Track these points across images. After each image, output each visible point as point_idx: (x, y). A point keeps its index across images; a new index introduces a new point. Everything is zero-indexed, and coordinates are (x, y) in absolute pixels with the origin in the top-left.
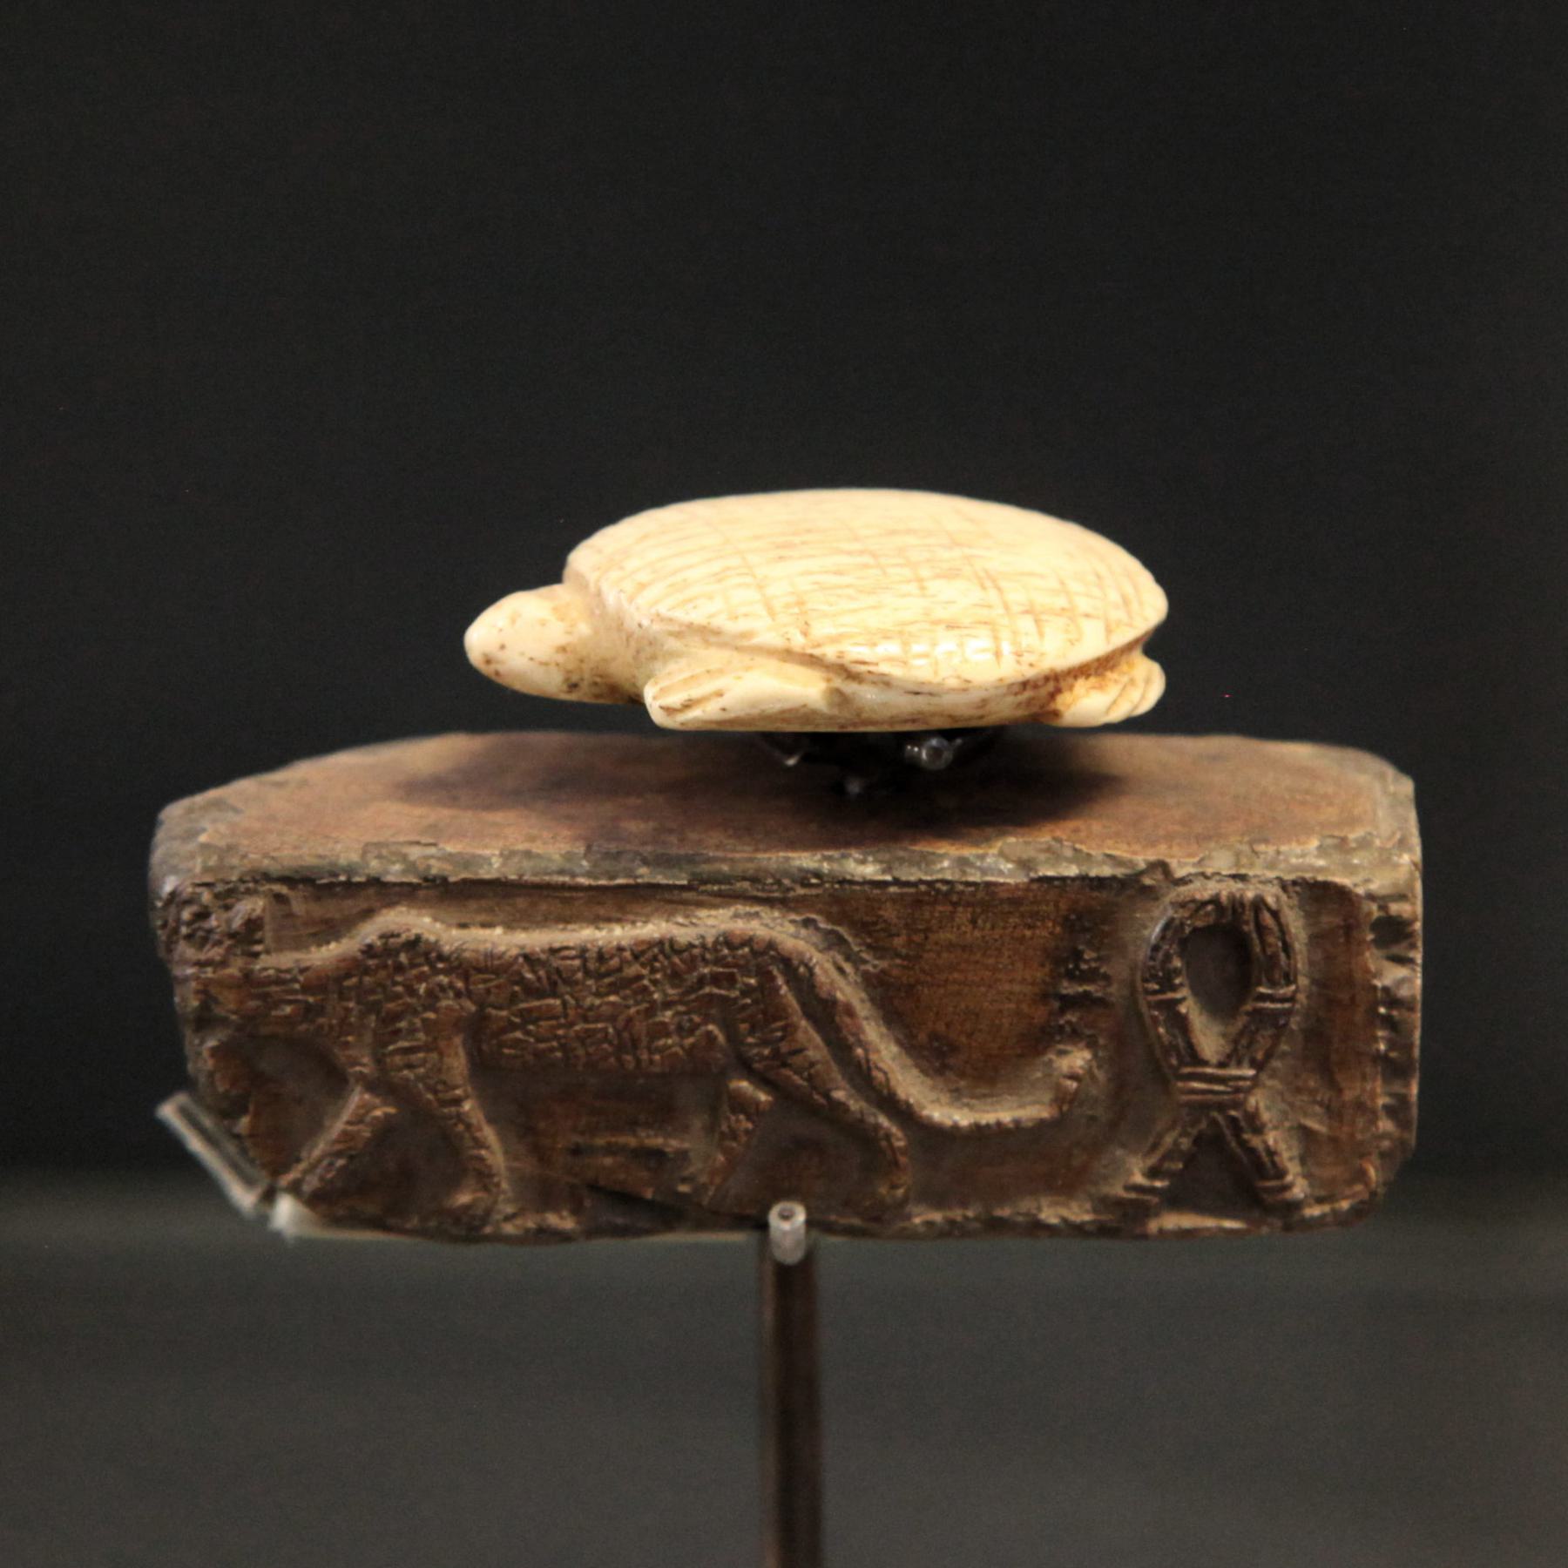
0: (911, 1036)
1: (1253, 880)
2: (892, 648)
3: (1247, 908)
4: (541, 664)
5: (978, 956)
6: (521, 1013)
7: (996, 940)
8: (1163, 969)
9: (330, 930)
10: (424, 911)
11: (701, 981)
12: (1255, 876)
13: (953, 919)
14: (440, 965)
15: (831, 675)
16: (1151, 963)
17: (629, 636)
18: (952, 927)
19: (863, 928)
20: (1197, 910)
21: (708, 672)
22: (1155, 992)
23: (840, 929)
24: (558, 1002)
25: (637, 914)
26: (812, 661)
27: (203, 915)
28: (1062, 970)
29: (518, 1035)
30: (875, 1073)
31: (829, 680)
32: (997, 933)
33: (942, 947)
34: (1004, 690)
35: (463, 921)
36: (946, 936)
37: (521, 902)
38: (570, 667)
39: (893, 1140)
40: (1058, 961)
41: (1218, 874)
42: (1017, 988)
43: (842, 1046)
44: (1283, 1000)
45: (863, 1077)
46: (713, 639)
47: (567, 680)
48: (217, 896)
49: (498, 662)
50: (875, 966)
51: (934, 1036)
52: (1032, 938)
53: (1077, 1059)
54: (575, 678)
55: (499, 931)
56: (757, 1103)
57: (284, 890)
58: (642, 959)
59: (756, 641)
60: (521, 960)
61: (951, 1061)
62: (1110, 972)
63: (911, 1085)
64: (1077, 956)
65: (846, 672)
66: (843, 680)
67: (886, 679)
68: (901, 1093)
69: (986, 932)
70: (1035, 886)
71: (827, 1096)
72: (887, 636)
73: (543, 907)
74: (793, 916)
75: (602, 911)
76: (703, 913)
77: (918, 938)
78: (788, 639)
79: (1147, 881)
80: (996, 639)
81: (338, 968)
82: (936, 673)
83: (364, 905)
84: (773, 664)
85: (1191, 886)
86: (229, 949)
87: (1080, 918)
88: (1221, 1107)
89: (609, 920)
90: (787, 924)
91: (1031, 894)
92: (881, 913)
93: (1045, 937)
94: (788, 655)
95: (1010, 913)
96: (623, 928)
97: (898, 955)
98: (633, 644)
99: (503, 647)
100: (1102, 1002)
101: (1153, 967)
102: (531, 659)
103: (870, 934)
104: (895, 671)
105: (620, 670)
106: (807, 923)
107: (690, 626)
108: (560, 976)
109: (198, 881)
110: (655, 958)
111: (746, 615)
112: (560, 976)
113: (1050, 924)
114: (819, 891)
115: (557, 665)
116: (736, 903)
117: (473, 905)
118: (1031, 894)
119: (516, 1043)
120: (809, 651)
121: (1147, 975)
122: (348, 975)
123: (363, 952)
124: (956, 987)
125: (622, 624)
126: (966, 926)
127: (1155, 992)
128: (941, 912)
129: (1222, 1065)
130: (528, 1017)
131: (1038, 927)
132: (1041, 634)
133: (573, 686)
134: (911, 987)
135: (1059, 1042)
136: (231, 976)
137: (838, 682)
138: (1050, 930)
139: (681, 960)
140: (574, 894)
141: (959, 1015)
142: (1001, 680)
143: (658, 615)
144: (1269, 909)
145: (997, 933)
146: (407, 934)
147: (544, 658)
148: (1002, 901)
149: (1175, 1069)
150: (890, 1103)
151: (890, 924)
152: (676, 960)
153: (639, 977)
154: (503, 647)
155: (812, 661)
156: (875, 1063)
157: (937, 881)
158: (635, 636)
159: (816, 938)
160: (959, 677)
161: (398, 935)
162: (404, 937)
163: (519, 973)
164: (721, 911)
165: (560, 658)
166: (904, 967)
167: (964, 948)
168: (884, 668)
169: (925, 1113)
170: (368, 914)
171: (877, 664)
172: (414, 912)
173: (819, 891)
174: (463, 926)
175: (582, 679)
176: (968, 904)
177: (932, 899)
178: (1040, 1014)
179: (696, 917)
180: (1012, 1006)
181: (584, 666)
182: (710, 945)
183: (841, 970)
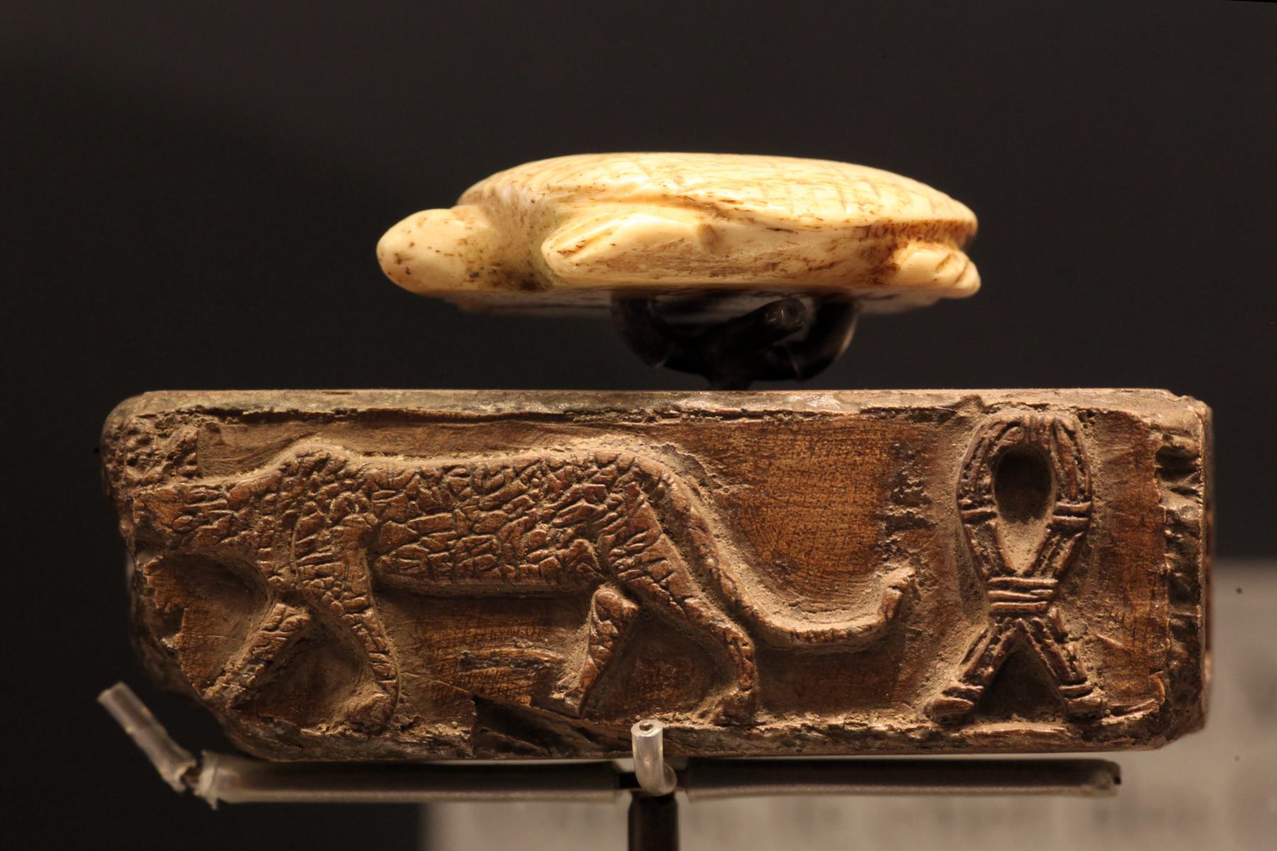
0: (757, 554)
1: (1052, 408)
2: (756, 193)
3: (1047, 429)
4: (446, 255)
5: (815, 480)
6: (416, 526)
7: (830, 466)
8: (975, 486)
9: (256, 459)
10: (335, 441)
11: (575, 498)
12: (1054, 405)
13: (793, 446)
14: (348, 482)
15: (703, 214)
16: (964, 480)
17: (523, 215)
18: (793, 453)
19: (715, 455)
20: (1004, 431)
21: (597, 220)
22: (968, 507)
23: (697, 457)
24: (449, 515)
25: (519, 442)
26: (688, 203)
27: (146, 442)
28: (889, 494)
29: (415, 546)
30: (724, 581)
31: (702, 218)
32: (832, 458)
33: (783, 472)
34: (848, 233)
35: (371, 449)
36: (786, 462)
37: (420, 432)
38: (472, 256)
39: (740, 644)
40: (884, 487)
41: (1024, 404)
42: (849, 509)
43: (696, 557)
44: (1078, 514)
45: (713, 583)
46: (599, 196)
47: (469, 269)
48: (158, 426)
49: (408, 259)
50: (726, 490)
51: (778, 554)
52: (861, 465)
53: (902, 573)
54: (476, 268)
55: (400, 458)
56: (621, 609)
57: (216, 420)
58: (523, 475)
59: (636, 192)
60: (418, 477)
61: (792, 578)
62: (929, 495)
63: (757, 597)
64: (902, 481)
65: (712, 208)
66: (714, 218)
67: (749, 215)
68: (747, 599)
69: (822, 458)
70: (865, 417)
71: (681, 601)
72: (748, 184)
73: (440, 438)
74: (655, 444)
75: (490, 441)
76: (576, 440)
77: (763, 463)
78: (664, 186)
79: (962, 413)
80: (840, 192)
81: (259, 485)
82: (792, 211)
83: (286, 436)
84: (653, 207)
85: (999, 413)
86: (166, 469)
87: (903, 445)
88: (1026, 613)
89: (495, 448)
90: (649, 449)
91: (861, 424)
92: (731, 440)
93: (873, 463)
94: (665, 199)
95: (844, 441)
96: (507, 454)
97: (746, 481)
98: (527, 220)
99: (412, 244)
100: (922, 524)
101: (966, 485)
102: (438, 251)
103: (721, 460)
104: (758, 209)
105: (514, 256)
106: (666, 450)
107: (578, 189)
108: (452, 491)
109: (142, 414)
110: (533, 475)
111: (626, 174)
112: (452, 491)
113: (878, 452)
114: (678, 421)
115: (461, 255)
116: (606, 433)
117: (379, 434)
118: (861, 424)
119: (413, 554)
120: (683, 194)
121: (961, 492)
122: (268, 491)
123: (283, 471)
124: (796, 509)
125: (516, 208)
126: (805, 453)
127: (968, 507)
128: (782, 440)
129: (1028, 574)
130: (424, 530)
131: (867, 455)
132: (878, 194)
133: (475, 276)
134: (758, 508)
135: (886, 560)
136: (167, 492)
137: (710, 220)
138: (878, 456)
139: (556, 476)
140: (465, 425)
141: (798, 534)
142: (848, 221)
143: (549, 188)
144: (1067, 431)
145: (832, 458)
146: (321, 453)
147: (450, 251)
148: (835, 430)
149: (985, 578)
150: (736, 610)
151: (739, 452)
152: (551, 475)
153: (522, 492)
154: (412, 244)
155: (688, 203)
156: (724, 573)
157: (779, 412)
158: (529, 212)
159: (674, 462)
160: (812, 216)
161: (312, 455)
162: (317, 457)
163: (416, 488)
164: (592, 439)
165: (462, 249)
166: (752, 491)
167: (802, 473)
168: (748, 206)
169: (767, 619)
170: (288, 443)
171: (741, 203)
172: (327, 441)
173: (678, 421)
174: (368, 454)
175: (482, 268)
176: (807, 433)
177: (775, 429)
178: (868, 534)
179: (571, 444)
180: (846, 526)
181: (485, 256)
182: (581, 463)
183: (695, 490)
